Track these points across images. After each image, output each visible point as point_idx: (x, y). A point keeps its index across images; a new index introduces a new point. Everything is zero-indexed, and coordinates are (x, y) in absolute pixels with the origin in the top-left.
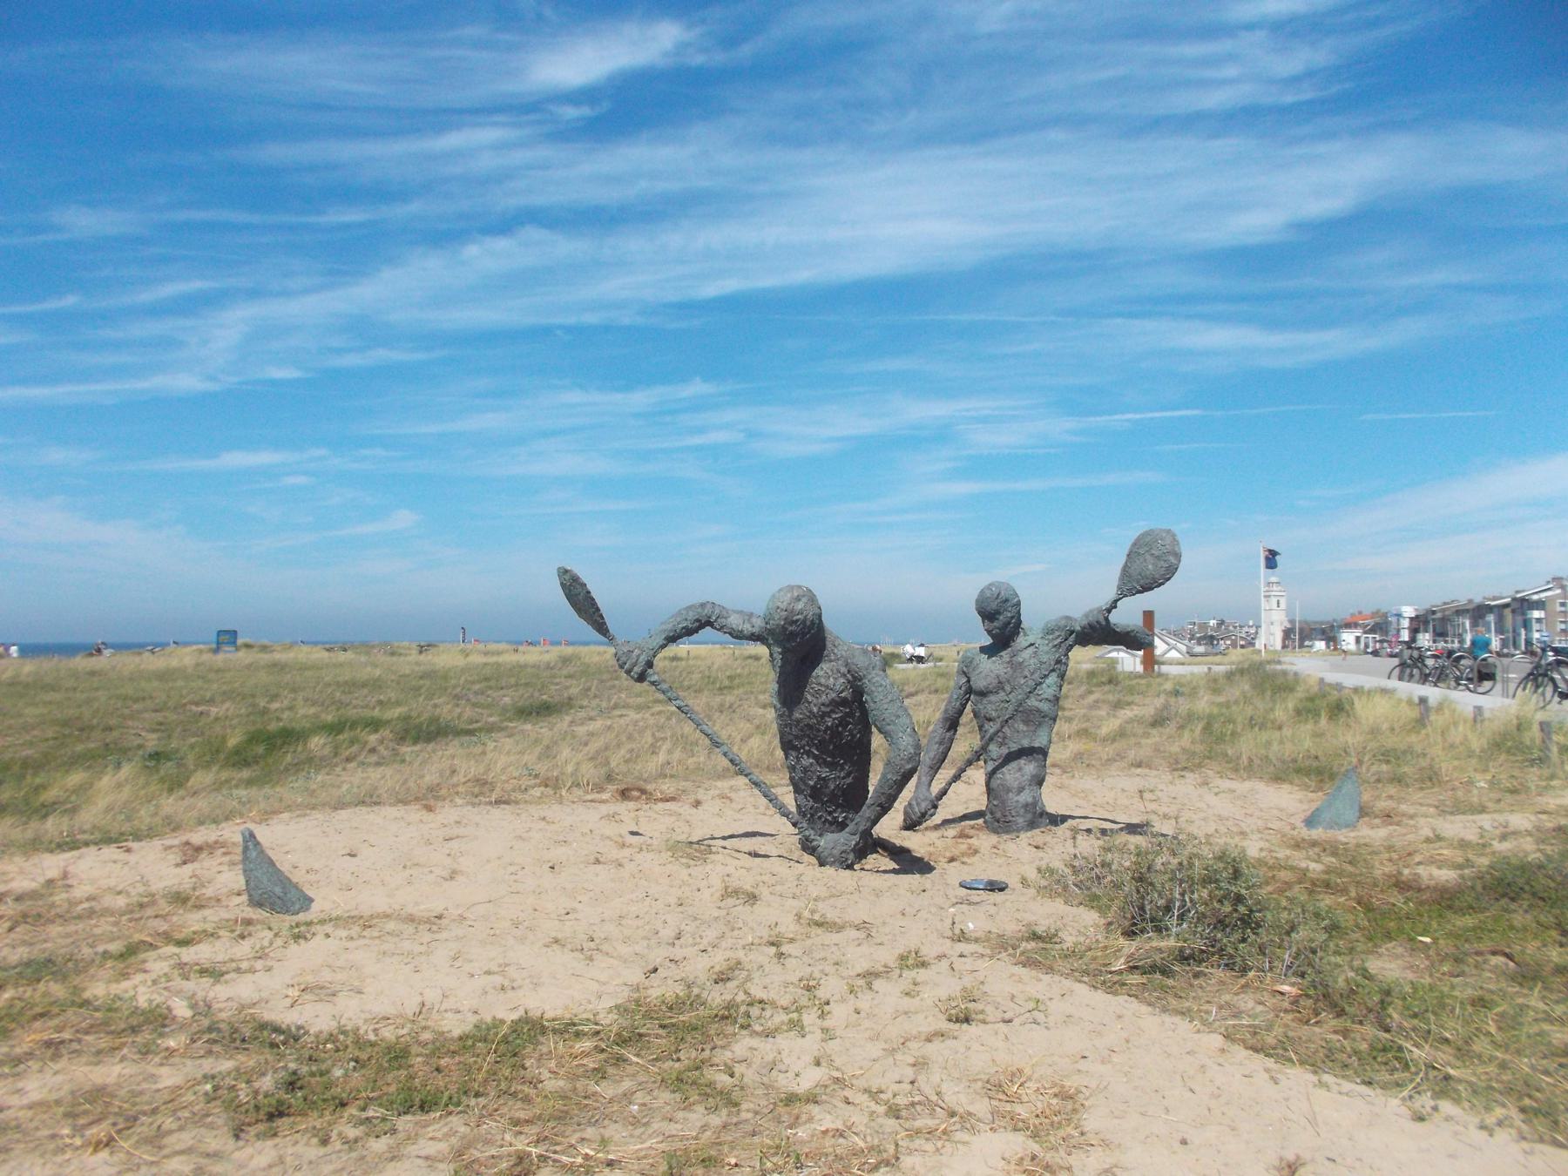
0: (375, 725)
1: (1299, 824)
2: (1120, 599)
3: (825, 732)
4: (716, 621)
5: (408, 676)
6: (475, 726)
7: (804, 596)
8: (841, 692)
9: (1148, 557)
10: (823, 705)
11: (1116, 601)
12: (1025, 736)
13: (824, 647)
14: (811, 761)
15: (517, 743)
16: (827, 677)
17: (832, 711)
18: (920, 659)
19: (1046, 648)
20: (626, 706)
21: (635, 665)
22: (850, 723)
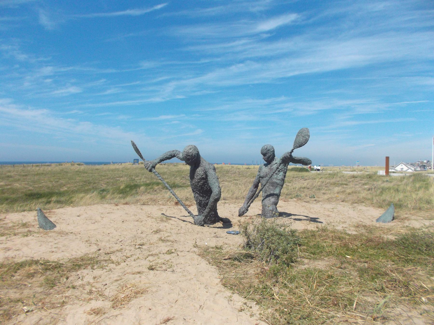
0: (158, 184)
1: (374, 220)
2: (294, 149)
3: (199, 187)
4: (176, 155)
5: (174, 171)
6: (185, 185)
7: (192, 148)
8: (203, 175)
9: (301, 136)
10: (198, 179)
11: (293, 150)
12: (272, 190)
13: (200, 163)
14: (198, 195)
16: (199, 171)
17: (200, 181)
18: (318, 170)
20: (227, 181)
21: (149, 167)
22: (206, 185)
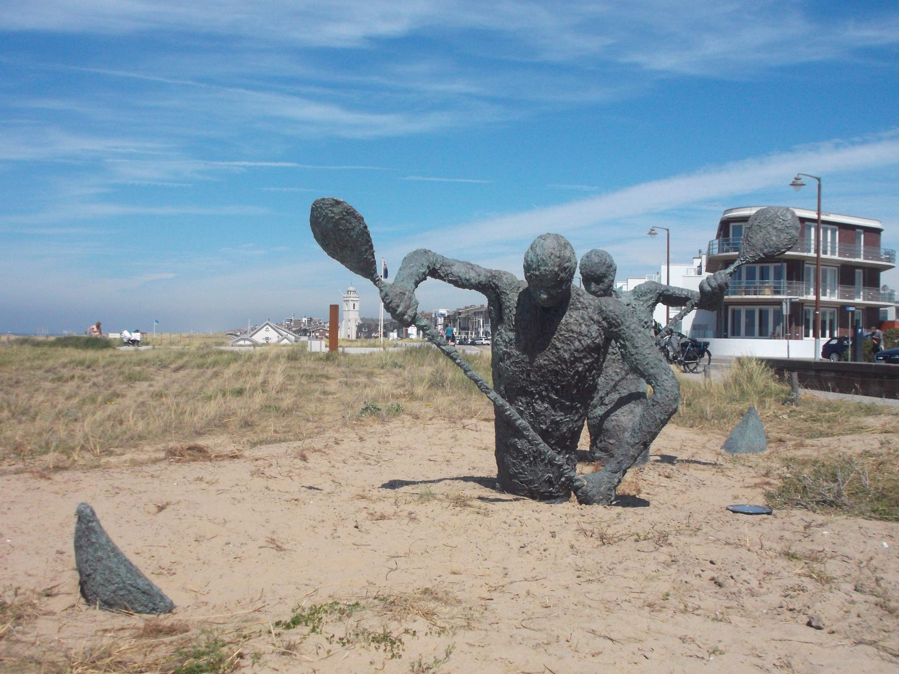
3: (573, 377)
14: (546, 405)
15: (36, 401)
17: (585, 357)
18: (134, 342)
19: (642, 308)
